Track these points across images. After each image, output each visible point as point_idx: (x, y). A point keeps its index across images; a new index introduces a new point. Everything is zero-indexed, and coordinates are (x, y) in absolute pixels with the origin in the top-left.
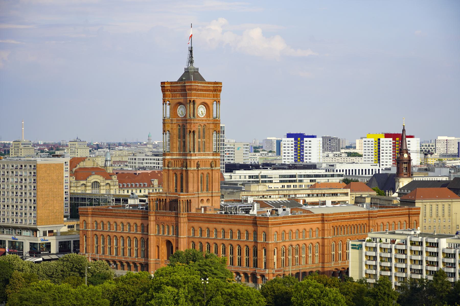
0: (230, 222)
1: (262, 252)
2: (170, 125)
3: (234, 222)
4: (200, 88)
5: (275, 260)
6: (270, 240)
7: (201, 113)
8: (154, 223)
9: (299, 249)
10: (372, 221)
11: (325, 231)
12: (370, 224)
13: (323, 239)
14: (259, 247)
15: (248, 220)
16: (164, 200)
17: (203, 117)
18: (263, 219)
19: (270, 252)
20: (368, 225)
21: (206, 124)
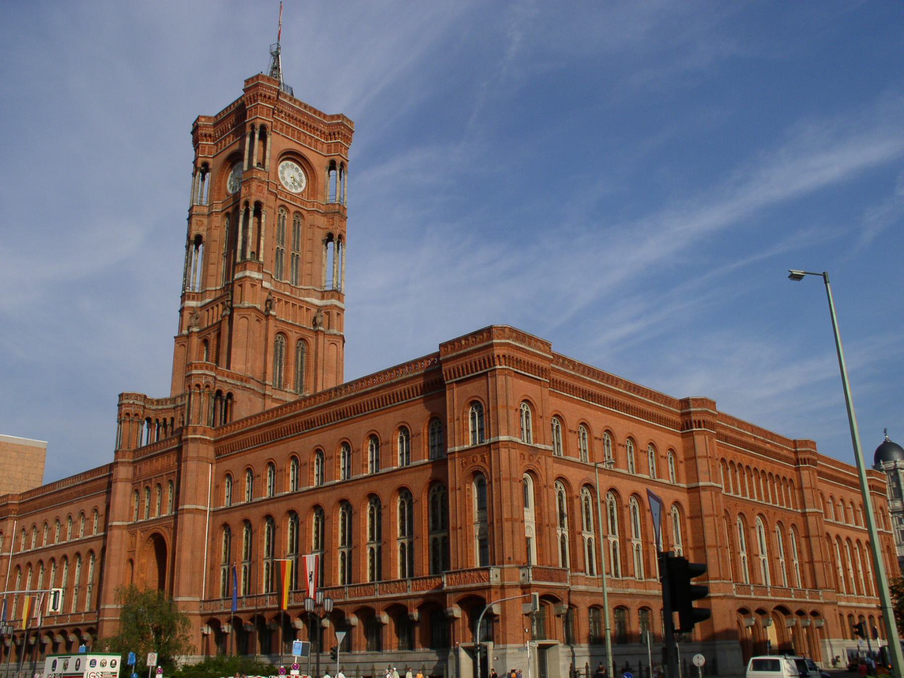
0: (341, 415)
1: (466, 497)
2: (205, 221)
3: (357, 410)
4: (286, 109)
5: (531, 531)
6: (502, 427)
7: (289, 181)
8: (129, 485)
9: (620, 510)
10: (807, 472)
11: (699, 460)
12: (804, 481)
13: (694, 491)
14: (455, 473)
15: (404, 381)
16: (169, 422)
17: (299, 194)
18: (467, 345)
19: (505, 485)
20: (796, 485)
21: (304, 212)
